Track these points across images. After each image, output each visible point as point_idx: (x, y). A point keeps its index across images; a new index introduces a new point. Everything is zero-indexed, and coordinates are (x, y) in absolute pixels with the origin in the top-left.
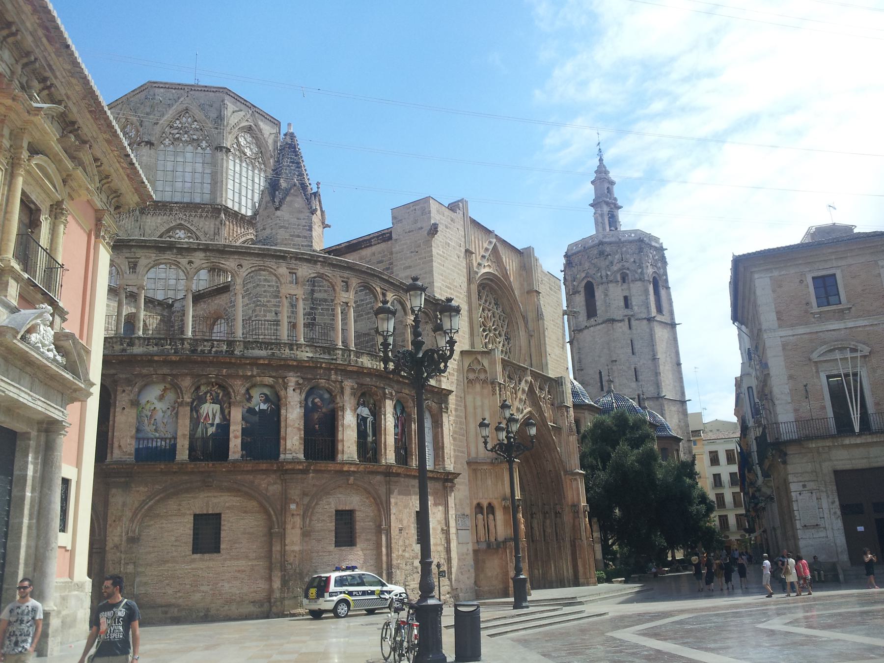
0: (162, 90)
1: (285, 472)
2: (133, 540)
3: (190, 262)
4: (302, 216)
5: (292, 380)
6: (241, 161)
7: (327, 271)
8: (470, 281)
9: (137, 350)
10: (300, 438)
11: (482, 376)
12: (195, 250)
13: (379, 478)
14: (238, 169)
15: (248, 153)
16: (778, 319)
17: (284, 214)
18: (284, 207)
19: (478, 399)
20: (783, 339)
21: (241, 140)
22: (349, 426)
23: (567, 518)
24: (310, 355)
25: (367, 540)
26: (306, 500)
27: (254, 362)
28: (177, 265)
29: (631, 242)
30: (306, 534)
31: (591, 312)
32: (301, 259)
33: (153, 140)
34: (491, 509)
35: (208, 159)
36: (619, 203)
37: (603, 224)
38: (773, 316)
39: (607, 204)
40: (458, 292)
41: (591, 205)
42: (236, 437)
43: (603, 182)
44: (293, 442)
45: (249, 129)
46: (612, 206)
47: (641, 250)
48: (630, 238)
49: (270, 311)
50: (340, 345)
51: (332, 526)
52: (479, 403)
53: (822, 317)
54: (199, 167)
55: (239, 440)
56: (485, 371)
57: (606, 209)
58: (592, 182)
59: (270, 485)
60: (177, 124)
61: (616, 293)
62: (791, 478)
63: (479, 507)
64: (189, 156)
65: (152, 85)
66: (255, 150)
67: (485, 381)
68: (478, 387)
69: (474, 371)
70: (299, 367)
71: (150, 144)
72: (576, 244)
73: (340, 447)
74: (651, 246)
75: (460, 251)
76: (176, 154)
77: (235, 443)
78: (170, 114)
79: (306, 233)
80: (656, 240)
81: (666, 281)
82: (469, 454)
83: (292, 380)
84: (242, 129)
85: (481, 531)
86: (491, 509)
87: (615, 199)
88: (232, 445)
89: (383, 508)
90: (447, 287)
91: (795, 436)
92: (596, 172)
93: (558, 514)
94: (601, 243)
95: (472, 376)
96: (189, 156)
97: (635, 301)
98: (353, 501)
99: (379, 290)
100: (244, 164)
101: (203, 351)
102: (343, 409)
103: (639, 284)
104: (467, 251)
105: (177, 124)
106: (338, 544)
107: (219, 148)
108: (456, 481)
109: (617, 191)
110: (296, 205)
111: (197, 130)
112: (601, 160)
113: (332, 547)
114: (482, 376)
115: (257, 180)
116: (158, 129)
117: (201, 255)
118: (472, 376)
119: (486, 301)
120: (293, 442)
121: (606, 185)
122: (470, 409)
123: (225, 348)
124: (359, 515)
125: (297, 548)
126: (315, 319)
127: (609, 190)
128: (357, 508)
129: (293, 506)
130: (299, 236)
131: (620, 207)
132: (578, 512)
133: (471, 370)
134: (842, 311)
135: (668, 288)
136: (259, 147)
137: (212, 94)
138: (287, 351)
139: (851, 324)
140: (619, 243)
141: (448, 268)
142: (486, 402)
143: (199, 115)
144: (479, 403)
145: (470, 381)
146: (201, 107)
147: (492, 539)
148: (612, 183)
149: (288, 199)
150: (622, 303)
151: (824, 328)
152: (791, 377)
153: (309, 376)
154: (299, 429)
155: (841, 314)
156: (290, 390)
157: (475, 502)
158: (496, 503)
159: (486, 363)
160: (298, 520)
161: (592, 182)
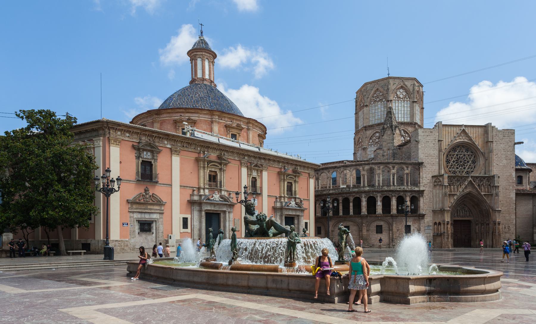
1: (362, 217)
9: (331, 192)
11: (440, 183)
14: (397, 105)
15: (401, 96)
17: (385, 137)
18: (385, 135)
21: (398, 93)
27: (354, 192)
35: (385, 105)
44: (364, 211)
50: (377, 184)
52: (438, 192)
54: (383, 109)
60: (375, 95)
64: (379, 106)
65: (366, 84)
66: (404, 94)
67: (440, 185)
68: (438, 187)
70: (365, 192)
76: (375, 106)
79: (392, 142)
83: (363, 195)
84: (399, 89)
95: (436, 184)
96: (379, 106)
100: (400, 101)
105: (375, 95)
107: (388, 101)
114: (440, 183)
115: (406, 105)
116: (369, 99)
118: (436, 184)
120: (364, 211)
122: (434, 194)
133: (435, 182)
136: (406, 92)
142: (441, 191)
145: (435, 185)
146: (382, 87)
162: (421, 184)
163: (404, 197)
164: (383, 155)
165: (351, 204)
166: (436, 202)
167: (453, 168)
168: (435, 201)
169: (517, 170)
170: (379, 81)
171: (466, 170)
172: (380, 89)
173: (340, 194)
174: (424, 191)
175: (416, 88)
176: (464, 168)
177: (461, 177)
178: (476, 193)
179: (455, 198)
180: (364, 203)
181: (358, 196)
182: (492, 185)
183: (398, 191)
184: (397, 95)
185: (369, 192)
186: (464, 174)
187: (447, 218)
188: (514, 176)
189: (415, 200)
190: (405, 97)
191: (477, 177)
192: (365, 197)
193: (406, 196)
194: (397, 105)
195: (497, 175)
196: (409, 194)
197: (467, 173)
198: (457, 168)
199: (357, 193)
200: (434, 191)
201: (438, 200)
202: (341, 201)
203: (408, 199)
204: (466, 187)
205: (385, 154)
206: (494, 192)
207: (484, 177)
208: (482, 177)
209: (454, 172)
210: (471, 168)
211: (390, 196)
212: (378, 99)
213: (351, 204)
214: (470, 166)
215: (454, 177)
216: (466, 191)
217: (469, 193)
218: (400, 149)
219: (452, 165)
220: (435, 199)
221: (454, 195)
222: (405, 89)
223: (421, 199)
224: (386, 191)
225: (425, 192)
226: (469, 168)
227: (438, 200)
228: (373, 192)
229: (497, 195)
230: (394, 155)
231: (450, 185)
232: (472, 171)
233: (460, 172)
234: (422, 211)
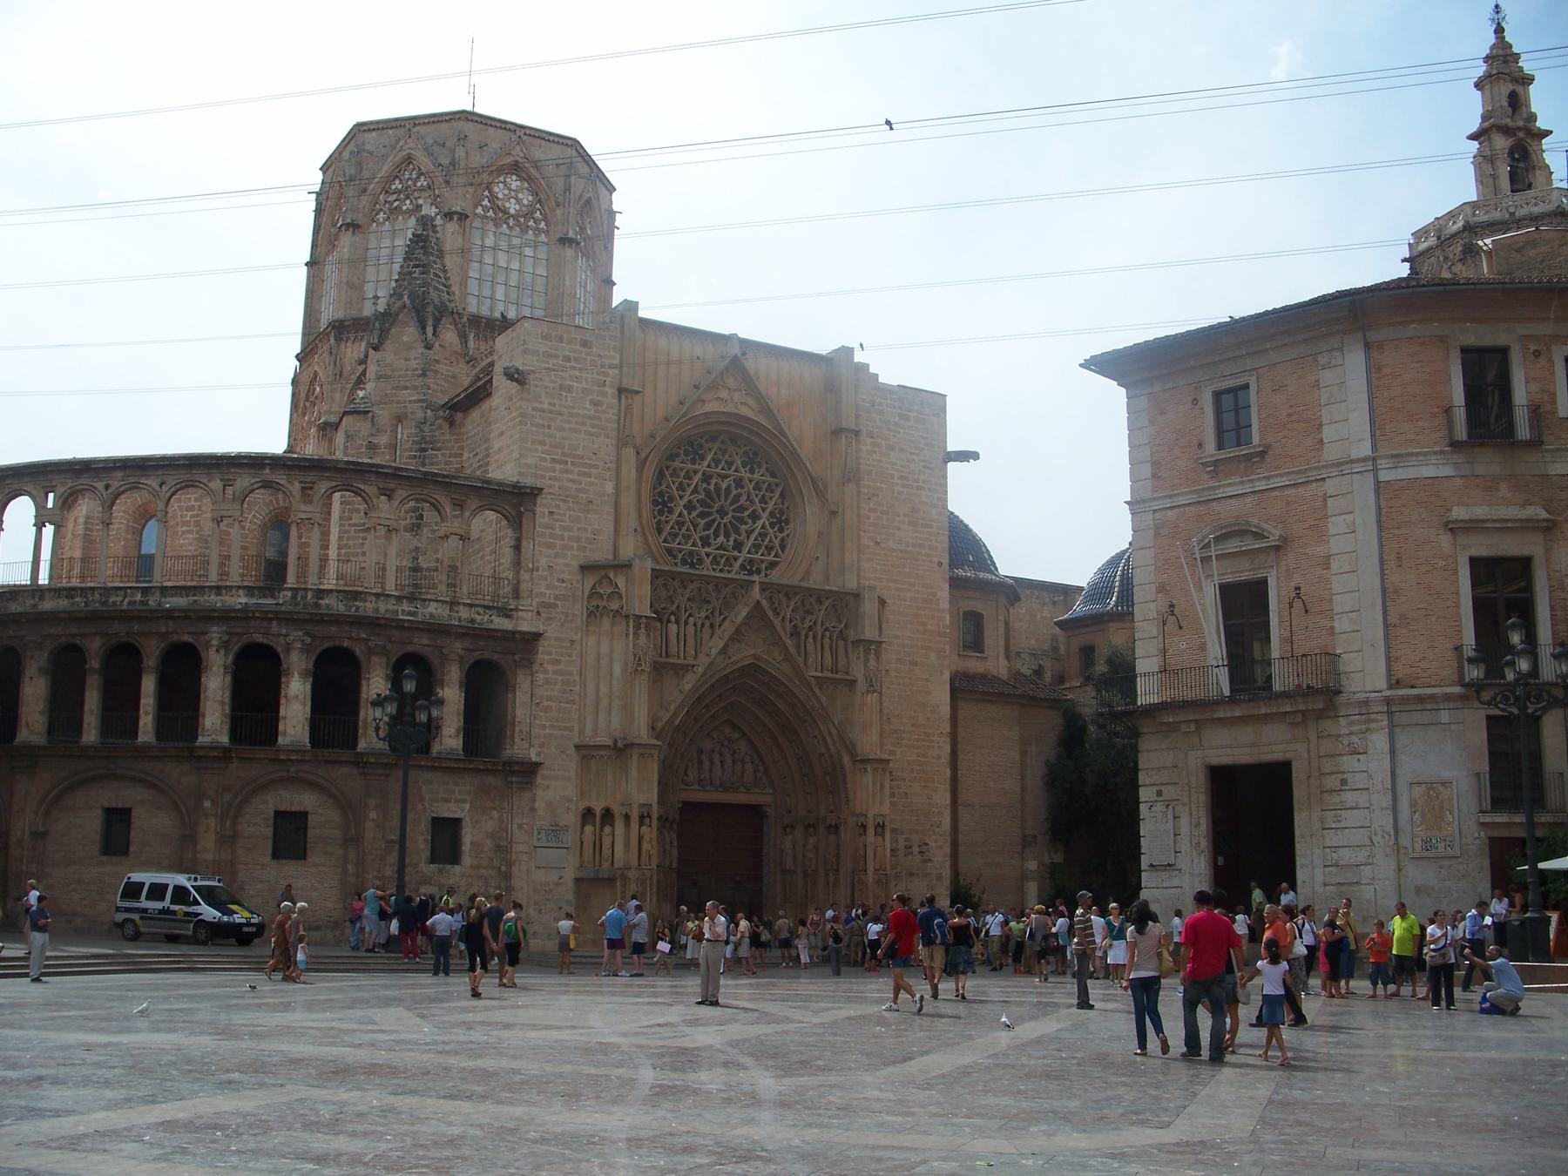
0: (374, 134)
2: (40, 836)
3: (107, 487)
4: (413, 354)
5: (216, 634)
6: (496, 225)
7: (281, 479)
8: (623, 441)
9: (47, 605)
10: (224, 715)
12: (114, 468)
13: (345, 770)
15: (513, 207)
16: (1154, 476)
18: (388, 345)
19: (605, 641)
20: (1157, 516)
21: (500, 191)
22: (296, 697)
24: (244, 600)
25: (326, 853)
26: (228, 797)
27: (169, 615)
28: (93, 489)
30: (228, 839)
32: (240, 465)
33: (360, 218)
34: (608, 816)
36: (1541, 124)
37: (1494, 177)
38: (1146, 471)
39: (1506, 131)
40: (585, 465)
41: (1472, 137)
42: (147, 713)
43: (1504, 77)
44: (214, 722)
45: (516, 169)
46: (1521, 135)
48: (1536, 210)
49: (358, 511)
51: (269, 832)
52: (605, 649)
55: (150, 718)
56: (620, 596)
57: (1501, 143)
58: (1478, 85)
59: (180, 775)
60: (397, 185)
62: (1143, 778)
63: (588, 814)
66: (527, 198)
68: (606, 623)
69: (601, 596)
70: (224, 616)
71: (353, 226)
73: (281, 727)
75: (604, 394)
78: (385, 169)
82: (581, 732)
83: (216, 634)
84: (501, 171)
85: (588, 850)
86: (608, 816)
87: (1533, 117)
88: (141, 723)
90: (553, 460)
91: (1154, 699)
92: (1487, 59)
93: (834, 829)
94: (1471, 229)
98: (305, 800)
99: (371, 490)
101: (114, 603)
102: (288, 673)
104: (620, 391)
105: (397, 185)
106: (276, 855)
108: (542, 772)
110: (405, 338)
111: (422, 189)
112: (1499, 30)
113: (267, 859)
114: (615, 606)
116: (365, 199)
117: (119, 474)
119: (717, 462)
120: (214, 722)
123: (139, 597)
124: (313, 820)
125: (210, 857)
126: (421, 517)
127: (1516, 102)
128: (309, 809)
129: (207, 804)
130: (406, 388)
131: (1548, 133)
132: (864, 826)
133: (593, 594)
134: (1248, 457)
137: (444, 126)
138: (213, 597)
139: (1260, 486)
141: (563, 429)
143: (425, 162)
144: (605, 649)
145: (591, 614)
147: (606, 865)
149: (393, 330)
151: (1220, 493)
152: (1162, 588)
153: (239, 630)
154: (222, 703)
156: (212, 651)
157: (582, 806)
158: (617, 811)
159: (621, 581)
160: (212, 822)
161: (1478, 85)
162: (525, 603)
163: (436, 662)
164: (372, 447)
165: (149, 685)
166: (598, 701)
167: (687, 537)
168: (590, 699)
169: (956, 583)
170: (415, 121)
171: (743, 556)
172: (420, 156)
173: (92, 617)
174: (537, 636)
175: (578, 185)
176: (738, 546)
177: (718, 584)
178: (786, 667)
179: (689, 682)
180: (216, 686)
181: (187, 638)
182: (852, 636)
183: (400, 626)
184: (493, 197)
185: (245, 615)
186: (735, 573)
187: (639, 787)
188: (945, 605)
189: (487, 685)
190: (529, 214)
191: (789, 592)
192: (225, 645)
193: (444, 659)
194: (489, 242)
195: (873, 588)
196: (458, 646)
197: (750, 567)
198: (705, 542)
199: (185, 616)
200: (591, 641)
201: (603, 689)
202: (95, 664)
204: (736, 637)
205: (383, 440)
206: (858, 672)
207: (820, 596)
208: (810, 592)
209: (692, 560)
210: (769, 549)
211: (358, 650)
212: (407, 205)
213: (149, 685)
214: (763, 535)
215: (685, 580)
216: (744, 654)
217: (754, 670)
218: (452, 423)
219: (680, 524)
220: (591, 686)
221: (681, 670)
222: (530, 179)
223: (522, 681)
224: (337, 620)
225: (542, 646)
226: (757, 547)
227: (603, 689)
228: (268, 616)
229: (871, 687)
230: (423, 447)
231: (661, 617)
232: (773, 565)
233: (715, 561)
234: (518, 749)
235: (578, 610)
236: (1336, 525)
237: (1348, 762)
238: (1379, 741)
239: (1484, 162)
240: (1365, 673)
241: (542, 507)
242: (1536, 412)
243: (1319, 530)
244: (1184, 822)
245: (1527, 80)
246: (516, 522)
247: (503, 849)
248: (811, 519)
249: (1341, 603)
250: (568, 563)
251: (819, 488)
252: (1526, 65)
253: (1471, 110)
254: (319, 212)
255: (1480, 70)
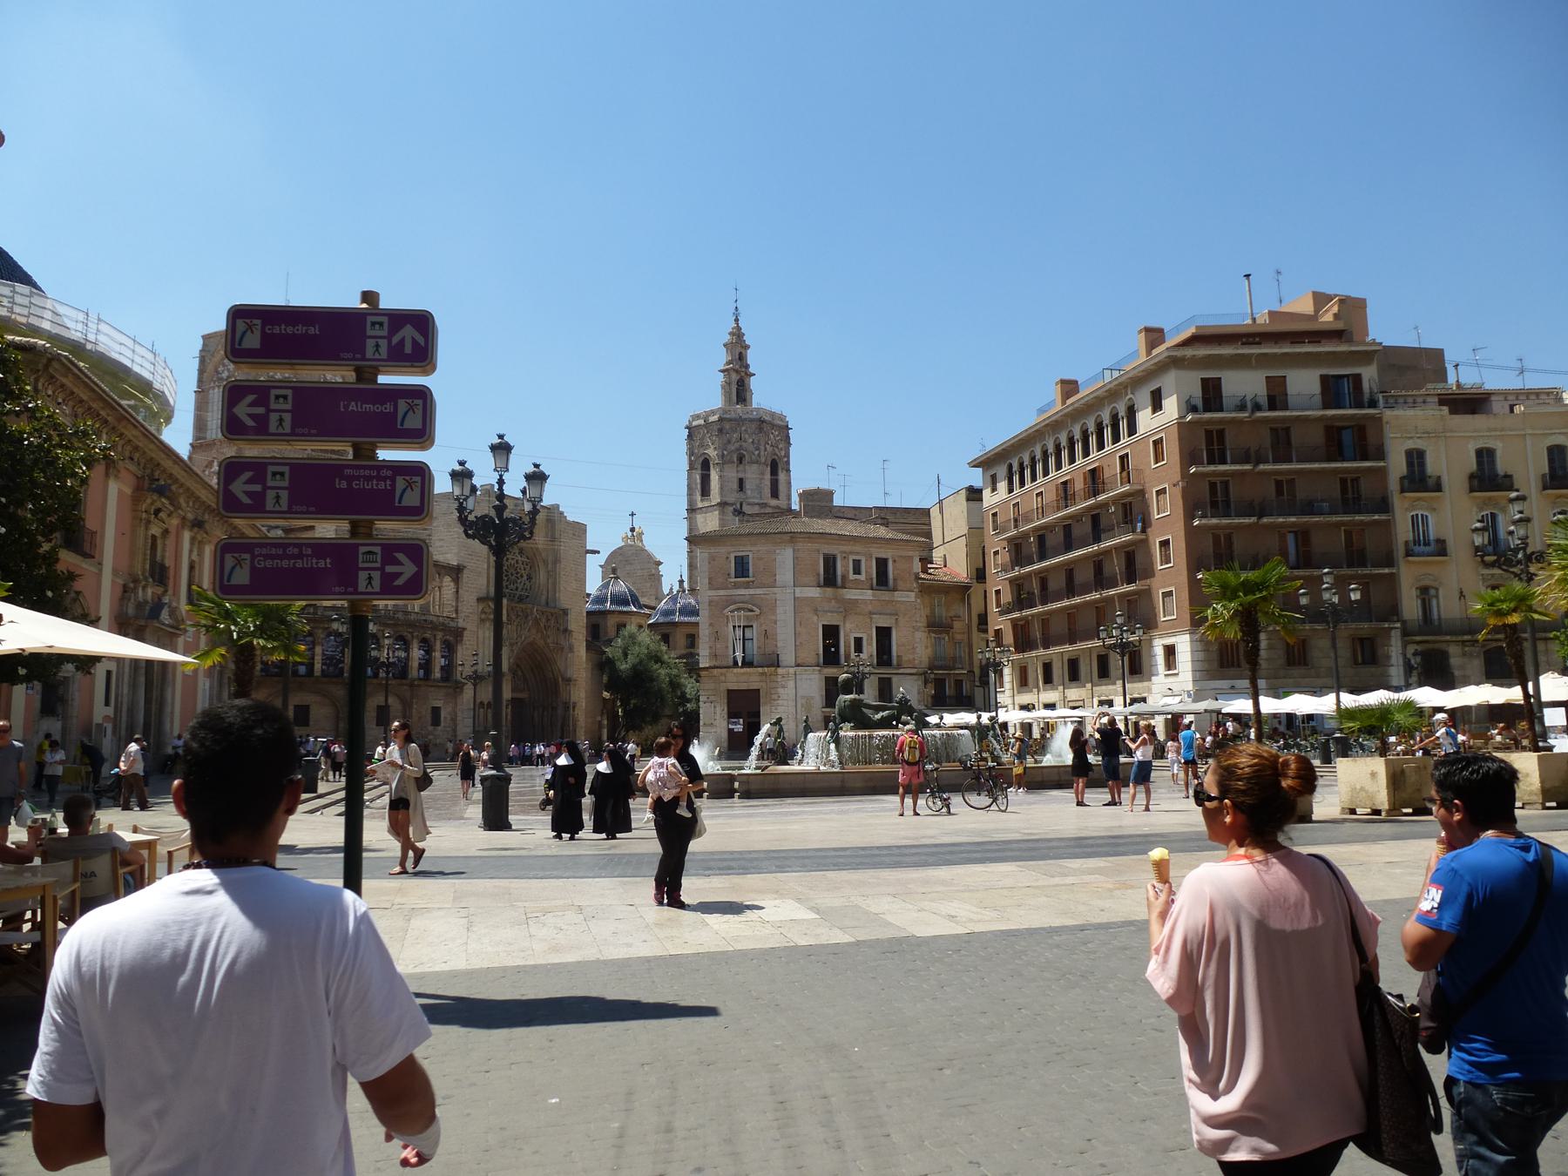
23: (560, 711)
29: (751, 420)
31: (705, 492)
36: (751, 370)
39: (737, 371)
47: (761, 429)
53: (736, 586)
57: (735, 377)
61: (732, 474)
72: (697, 417)
74: (773, 426)
77: (318, 666)
80: (782, 418)
81: (788, 463)
87: (747, 366)
89: (406, 705)
97: (748, 485)
103: (755, 467)
109: (752, 358)
112: (737, 320)
121: (739, 350)
127: (742, 357)
133: (483, 612)
135: (788, 471)
140: (739, 421)
145: (482, 621)
148: (747, 347)
150: (736, 486)
155: (747, 586)
189: (450, 649)
203: (438, 645)
235: (476, 618)
236: (779, 610)
237: (781, 690)
238: (791, 684)
239: (726, 386)
240: (788, 657)
241: (466, 574)
242: (844, 577)
243: (773, 608)
244: (718, 710)
245: (747, 347)
246: (457, 580)
247: (454, 720)
248: (542, 576)
249: (779, 637)
250: (473, 598)
251: (545, 562)
252: (748, 340)
253: (721, 358)
254: (203, 360)
255: (727, 338)
